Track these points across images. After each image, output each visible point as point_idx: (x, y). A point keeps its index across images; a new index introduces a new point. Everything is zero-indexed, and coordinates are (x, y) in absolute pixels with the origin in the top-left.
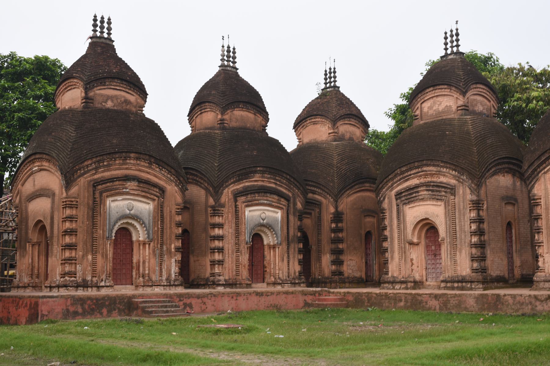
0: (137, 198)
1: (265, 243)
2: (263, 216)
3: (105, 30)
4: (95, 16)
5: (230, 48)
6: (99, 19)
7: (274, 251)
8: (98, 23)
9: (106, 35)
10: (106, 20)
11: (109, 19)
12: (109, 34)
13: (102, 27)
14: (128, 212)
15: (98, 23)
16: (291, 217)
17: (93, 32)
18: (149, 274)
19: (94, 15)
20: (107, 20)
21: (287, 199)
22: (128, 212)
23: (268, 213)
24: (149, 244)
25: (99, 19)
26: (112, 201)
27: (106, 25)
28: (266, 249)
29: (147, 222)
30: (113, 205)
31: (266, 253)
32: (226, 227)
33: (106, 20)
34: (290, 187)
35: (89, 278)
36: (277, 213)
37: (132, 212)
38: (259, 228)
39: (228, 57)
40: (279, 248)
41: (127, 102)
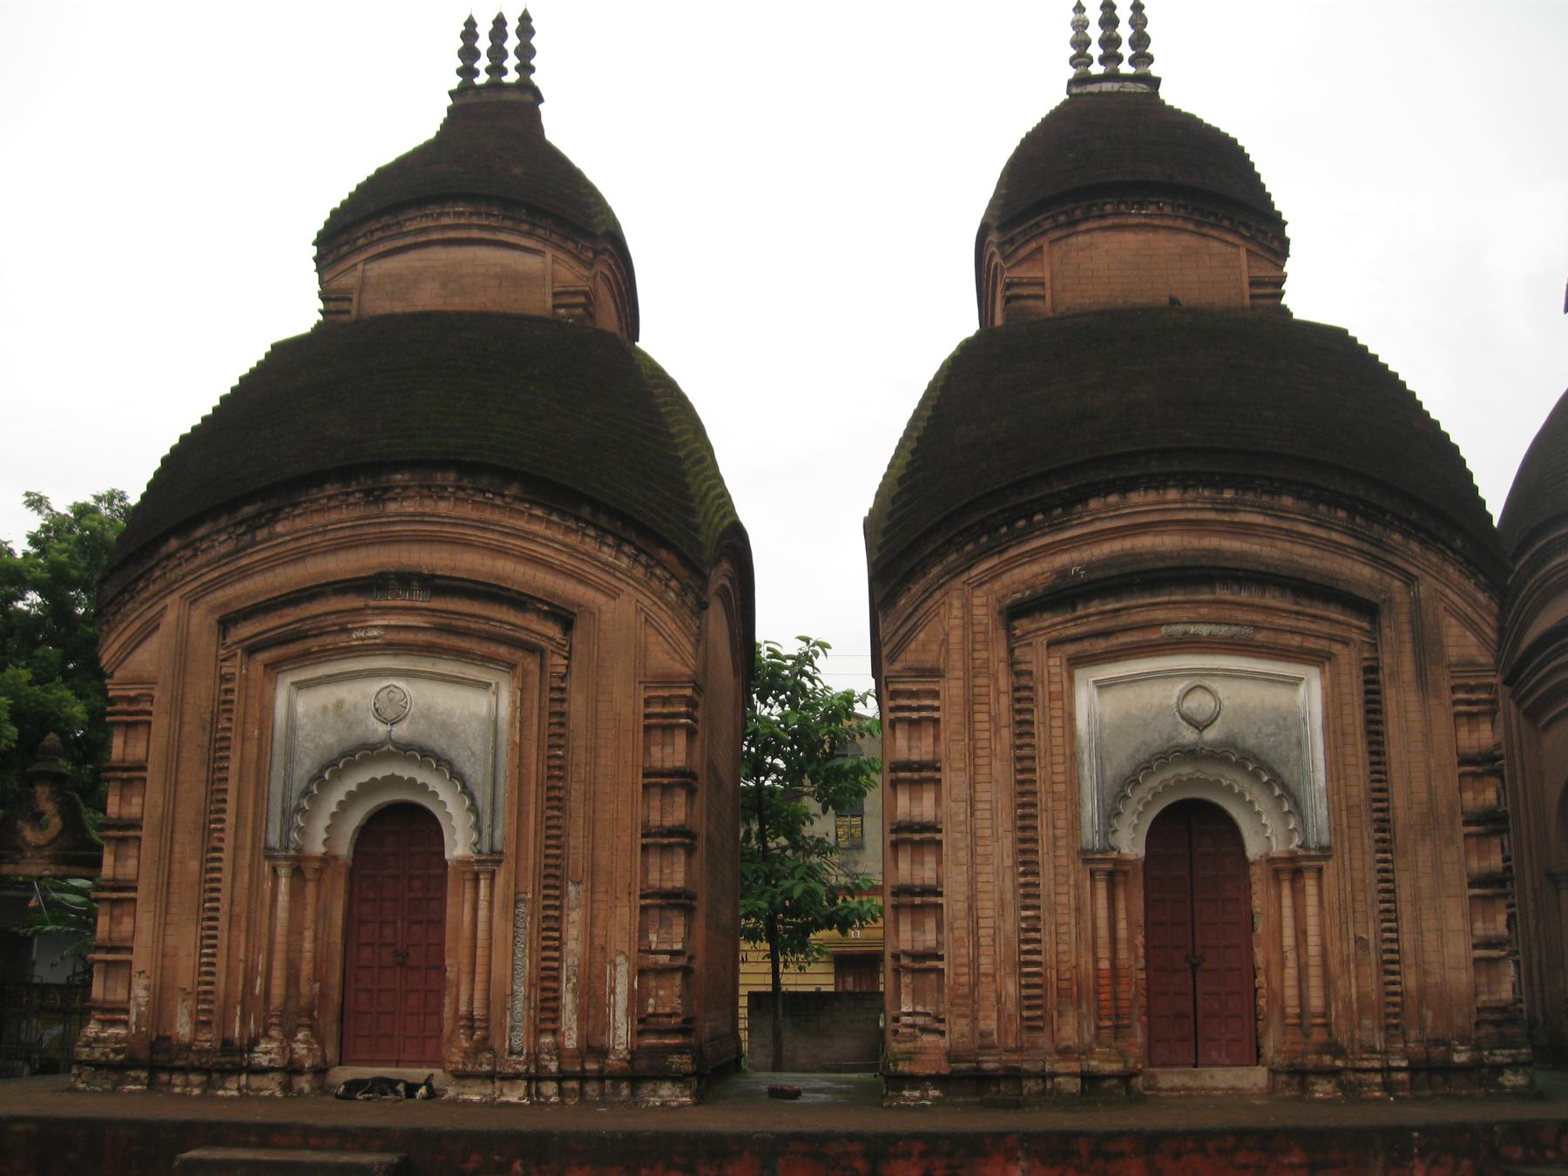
0: (425, 665)
1: (1253, 849)
2: (1199, 704)
3: (511, 62)
4: (471, 24)
5: (1114, 7)
6: (484, 29)
7: (1298, 893)
8: (483, 44)
9: (512, 77)
10: (512, 26)
11: (525, 19)
12: (525, 68)
13: (497, 53)
14: (382, 729)
15: (483, 44)
16: (1401, 703)
17: (460, 79)
18: (487, 1020)
19: (466, 18)
20: (517, 24)
21: (1367, 608)
22: (382, 729)
23: (1227, 692)
24: (493, 874)
25: (484, 29)
26: (301, 686)
27: (512, 43)
28: (1257, 874)
29: (476, 773)
30: (309, 705)
31: (1258, 903)
32: (956, 780)
33: (512, 26)
34: (1378, 543)
35: (183, 1028)
36: (1295, 682)
37: (402, 731)
38: (1186, 770)
39: (1110, 42)
40: (1320, 870)
41: (517, 280)
